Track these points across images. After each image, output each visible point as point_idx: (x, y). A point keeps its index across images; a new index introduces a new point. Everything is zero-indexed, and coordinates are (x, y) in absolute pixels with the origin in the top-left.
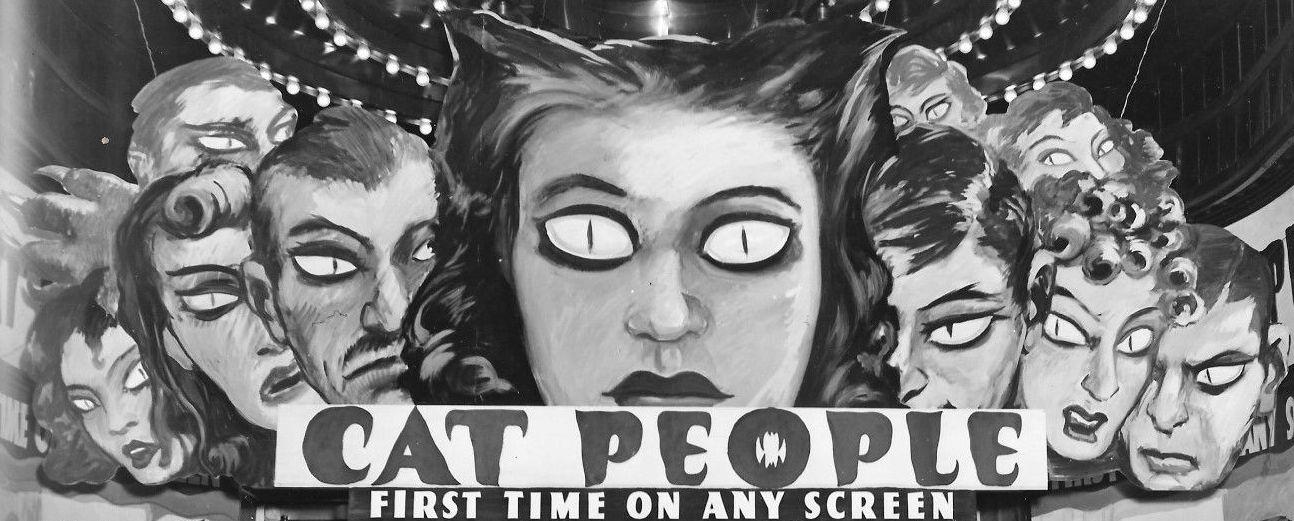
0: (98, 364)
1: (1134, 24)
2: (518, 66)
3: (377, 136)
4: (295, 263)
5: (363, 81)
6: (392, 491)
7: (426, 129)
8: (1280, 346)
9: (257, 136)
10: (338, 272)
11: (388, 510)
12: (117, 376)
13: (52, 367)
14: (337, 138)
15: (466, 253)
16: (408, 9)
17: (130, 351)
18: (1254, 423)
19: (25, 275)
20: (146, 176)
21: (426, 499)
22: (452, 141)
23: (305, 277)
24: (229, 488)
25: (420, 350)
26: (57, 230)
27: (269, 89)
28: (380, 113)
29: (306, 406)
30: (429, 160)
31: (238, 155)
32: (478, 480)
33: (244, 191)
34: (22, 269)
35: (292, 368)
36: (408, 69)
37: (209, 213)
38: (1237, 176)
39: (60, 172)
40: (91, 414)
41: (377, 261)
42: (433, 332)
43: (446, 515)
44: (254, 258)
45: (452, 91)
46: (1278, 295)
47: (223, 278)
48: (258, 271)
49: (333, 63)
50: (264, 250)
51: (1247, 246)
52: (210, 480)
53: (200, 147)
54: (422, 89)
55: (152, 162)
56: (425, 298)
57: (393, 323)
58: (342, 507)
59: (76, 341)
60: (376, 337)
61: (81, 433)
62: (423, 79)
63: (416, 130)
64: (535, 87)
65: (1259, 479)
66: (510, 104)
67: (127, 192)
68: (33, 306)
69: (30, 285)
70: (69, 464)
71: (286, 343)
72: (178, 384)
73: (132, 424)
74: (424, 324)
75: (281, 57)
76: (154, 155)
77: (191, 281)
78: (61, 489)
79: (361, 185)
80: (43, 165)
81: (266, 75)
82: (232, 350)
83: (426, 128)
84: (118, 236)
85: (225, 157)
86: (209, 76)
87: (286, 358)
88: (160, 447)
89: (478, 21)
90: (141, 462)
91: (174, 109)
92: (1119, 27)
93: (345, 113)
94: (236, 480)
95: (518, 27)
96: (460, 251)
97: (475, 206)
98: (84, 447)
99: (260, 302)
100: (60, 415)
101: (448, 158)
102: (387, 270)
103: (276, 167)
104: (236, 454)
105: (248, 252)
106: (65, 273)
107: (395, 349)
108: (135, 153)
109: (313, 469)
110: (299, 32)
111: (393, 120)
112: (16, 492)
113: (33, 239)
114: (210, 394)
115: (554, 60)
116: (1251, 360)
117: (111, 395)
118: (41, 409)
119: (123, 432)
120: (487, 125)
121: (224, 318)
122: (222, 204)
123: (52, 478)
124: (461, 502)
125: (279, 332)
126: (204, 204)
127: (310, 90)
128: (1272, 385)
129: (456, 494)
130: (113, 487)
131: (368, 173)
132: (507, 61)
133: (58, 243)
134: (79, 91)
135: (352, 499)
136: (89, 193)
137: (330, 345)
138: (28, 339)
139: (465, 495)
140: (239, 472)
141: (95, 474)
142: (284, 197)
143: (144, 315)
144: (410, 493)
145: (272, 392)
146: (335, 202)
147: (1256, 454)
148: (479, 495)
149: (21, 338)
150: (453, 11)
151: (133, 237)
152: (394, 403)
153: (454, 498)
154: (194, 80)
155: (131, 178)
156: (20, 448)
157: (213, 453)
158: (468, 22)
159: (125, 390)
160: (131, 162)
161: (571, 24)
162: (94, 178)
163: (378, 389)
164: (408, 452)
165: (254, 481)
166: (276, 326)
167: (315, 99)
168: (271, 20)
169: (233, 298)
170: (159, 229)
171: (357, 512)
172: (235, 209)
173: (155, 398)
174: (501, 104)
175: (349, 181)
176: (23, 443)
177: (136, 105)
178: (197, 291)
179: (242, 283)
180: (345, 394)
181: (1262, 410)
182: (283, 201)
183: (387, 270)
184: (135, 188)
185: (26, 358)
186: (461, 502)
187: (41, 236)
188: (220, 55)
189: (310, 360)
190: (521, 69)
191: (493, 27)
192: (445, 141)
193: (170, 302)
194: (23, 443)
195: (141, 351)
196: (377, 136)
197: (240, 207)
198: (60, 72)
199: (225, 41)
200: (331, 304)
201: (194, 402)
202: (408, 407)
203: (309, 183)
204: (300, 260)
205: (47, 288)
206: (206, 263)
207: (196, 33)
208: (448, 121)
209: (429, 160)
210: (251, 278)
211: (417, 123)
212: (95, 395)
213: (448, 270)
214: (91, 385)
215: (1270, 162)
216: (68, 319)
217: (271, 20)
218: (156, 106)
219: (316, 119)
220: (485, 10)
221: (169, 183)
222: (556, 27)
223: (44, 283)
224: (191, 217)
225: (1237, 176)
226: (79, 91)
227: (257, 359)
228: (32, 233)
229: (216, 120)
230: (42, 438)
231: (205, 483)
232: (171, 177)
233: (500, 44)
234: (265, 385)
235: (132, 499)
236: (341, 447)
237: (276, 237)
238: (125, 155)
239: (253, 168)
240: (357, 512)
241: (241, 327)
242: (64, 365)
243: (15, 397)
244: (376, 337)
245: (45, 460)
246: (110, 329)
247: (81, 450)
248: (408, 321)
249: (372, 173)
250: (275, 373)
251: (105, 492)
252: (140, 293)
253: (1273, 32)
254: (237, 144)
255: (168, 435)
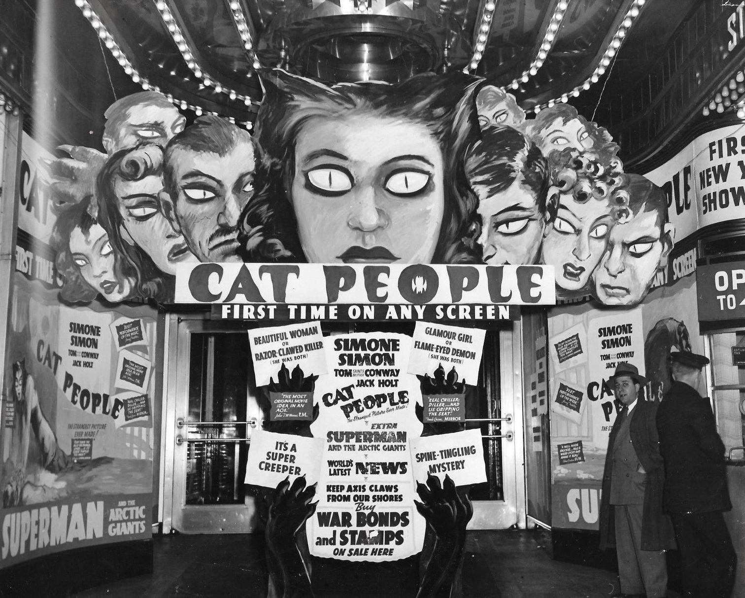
0: (88, 242)
1: (598, 75)
2: (295, 96)
3: (225, 130)
4: (185, 193)
5: (218, 103)
6: (232, 305)
7: (249, 127)
8: (670, 233)
9: (166, 130)
10: (206, 197)
11: (231, 314)
12: (97, 249)
13: (65, 244)
14: (206, 131)
15: (269, 188)
16: (240, 67)
17: (103, 236)
18: (657, 272)
19: (52, 199)
20: (111, 150)
21: (249, 309)
22: (262, 133)
23: (190, 200)
24: (152, 304)
25: (246, 236)
26: (67, 177)
27: (172, 107)
28: (227, 119)
29: (190, 263)
30: (251, 142)
31: (157, 140)
32: (275, 300)
33: (159, 157)
34: (50, 196)
35: (183, 244)
36: (240, 97)
37: (142, 168)
38: (649, 150)
39: (69, 148)
40: (84, 267)
41: (225, 192)
42: (253, 227)
43: (259, 317)
44: (164, 190)
45: (262, 108)
46: (669, 209)
47: (149, 200)
48: (166, 197)
49: (204, 94)
50: (170, 186)
51: (654, 184)
52: (143, 300)
53: (138, 135)
54: (247, 107)
55: (114, 143)
56: (249, 210)
57: (233, 223)
58: (208, 313)
59: (77, 231)
60: (225, 229)
61: (79, 276)
62: (248, 102)
63: (244, 127)
64: (303, 106)
65: (660, 299)
66: (291, 114)
67: (102, 158)
68: (56, 214)
69: (54, 204)
70: (73, 292)
71: (180, 232)
72: (127, 253)
73: (104, 272)
74: (248, 223)
75: (178, 91)
76: (116, 140)
77: (134, 202)
78: (69, 304)
79: (218, 154)
80: (60, 144)
81: (170, 100)
82: (154, 236)
83: (249, 126)
84: (97, 179)
85: (150, 140)
86: (142, 101)
87: (180, 240)
88: (118, 283)
89: (275, 73)
90: (109, 291)
91: (125, 117)
92: (591, 76)
93: (209, 119)
94: (156, 300)
95: (295, 76)
96: (266, 187)
97: (273, 165)
98: (81, 283)
99: (168, 212)
100: (69, 268)
101: (260, 141)
102: (230, 196)
103: (176, 146)
104: (155, 287)
105: (162, 187)
106: (71, 198)
107: (234, 235)
108: (106, 139)
109: (194, 294)
110: (187, 79)
111: (233, 122)
112: (47, 306)
113: (56, 181)
114: (143, 257)
115: (312, 93)
116: (656, 241)
117: (94, 258)
118: (59, 265)
119: (100, 276)
120: (279, 125)
121: (150, 220)
122: (149, 164)
123: (65, 299)
124: (267, 311)
125: (177, 227)
126: (140, 164)
127: (192, 107)
128: (666, 253)
129: (264, 307)
130: (95, 303)
131: (221, 148)
132: (289, 93)
133: (68, 183)
134: (78, 108)
135: (213, 309)
136: (83, 158)
137: (202, 233)
138: (53, 230)
139: (268, 307)
140: (157, 296)
141: (86, 297)
142: (179, 160)
143: (110, 218)
144: (241, 306)
145: (174, 256)
146: (205, 163)
147: (658, 287)
148: (275, 307)
149: (50, 230)
150: (263, 69)
151: (105, 180)
152: (233, 262)
153: (263, 309)
154: (135, 103)
155: (104, 151)
156: (49, 284)
157: (144, 286)
158: (270, 74)
159: (101, 255)
160: (104, 143)
161: (321, 75)
162: (86, 151)
163: (226, 255)
164: (240, 286)
165: (164, 300)
166: (175, 224)
167: (195, 112)
168: (173, 73)
169: (154, 210)
170: (118, 176)
171: (216, 315)
172: (155, 166)
173: (116, 259)
174: (286, 114)
175: (211, 152)
176: (51, 281)
177: (106, 115)
178: (137, 206)
179: (159, 202)
180: (209, 257)
181: (661, 265)
182: (179, 162)
183: (230, 196)
184: (106, 156)
185: (52, 240)
186: (267, 311)
187: (60, 179)
188: (148, 90)
189: (192, 241)
190: (296, 97)
191: (282, 76)
192: (259, 132)
193: (123, 212)
194: (51, 281)
195: (109, 236)
196: (225, 130)
197: (157, 165)
198: (69, 98)
199: (150, 83)
200: (203, 213)
201: (135, 261)
202: (241, 264)
203: (191, 154)
204: (187, 191)
205: (63, 205)
206: (141, 193)
207: (136, 79)
208: (260, 123)
209: (251, 142)
210: (163, 200)
211: (245, 124)
212: (86, 258)
213: (260, 196)
214: (84, 253)
215: (665, 143)
216: (73, 221)
217: (173, 73)
218: (117, 115)
219: (195, 122)
220: (279, 68)
221: (123, 153)
222: (314, 76)
223: (61, 203)
224: (134, 170)
225: (649, 150)
226: (78, 108)
227: (166, 240)
228: (55, 178)
229: (146, 122)
230: (60, 279)
231: (140, 301)
232: (124, 150)
233: (286, 85)
234: (170, 253)
235: (104, 309)
236: (207, 284)
237: (176, 180)
238: (101, 140)
239: (164, 146)
240: (216, 315)
241: (158, 224)
242: (71, 243)
243: (47, 259)
244: (225, 229)
245: (62, 290)
246: (94, 225)
247: (79, 285)
248: (240, 221)
249: (223, 148)
250: (175, 247)
251: (91, 306)
252: (108, 208)
253: (667, 79)
254: (156, 134)
255: (122, 277)
